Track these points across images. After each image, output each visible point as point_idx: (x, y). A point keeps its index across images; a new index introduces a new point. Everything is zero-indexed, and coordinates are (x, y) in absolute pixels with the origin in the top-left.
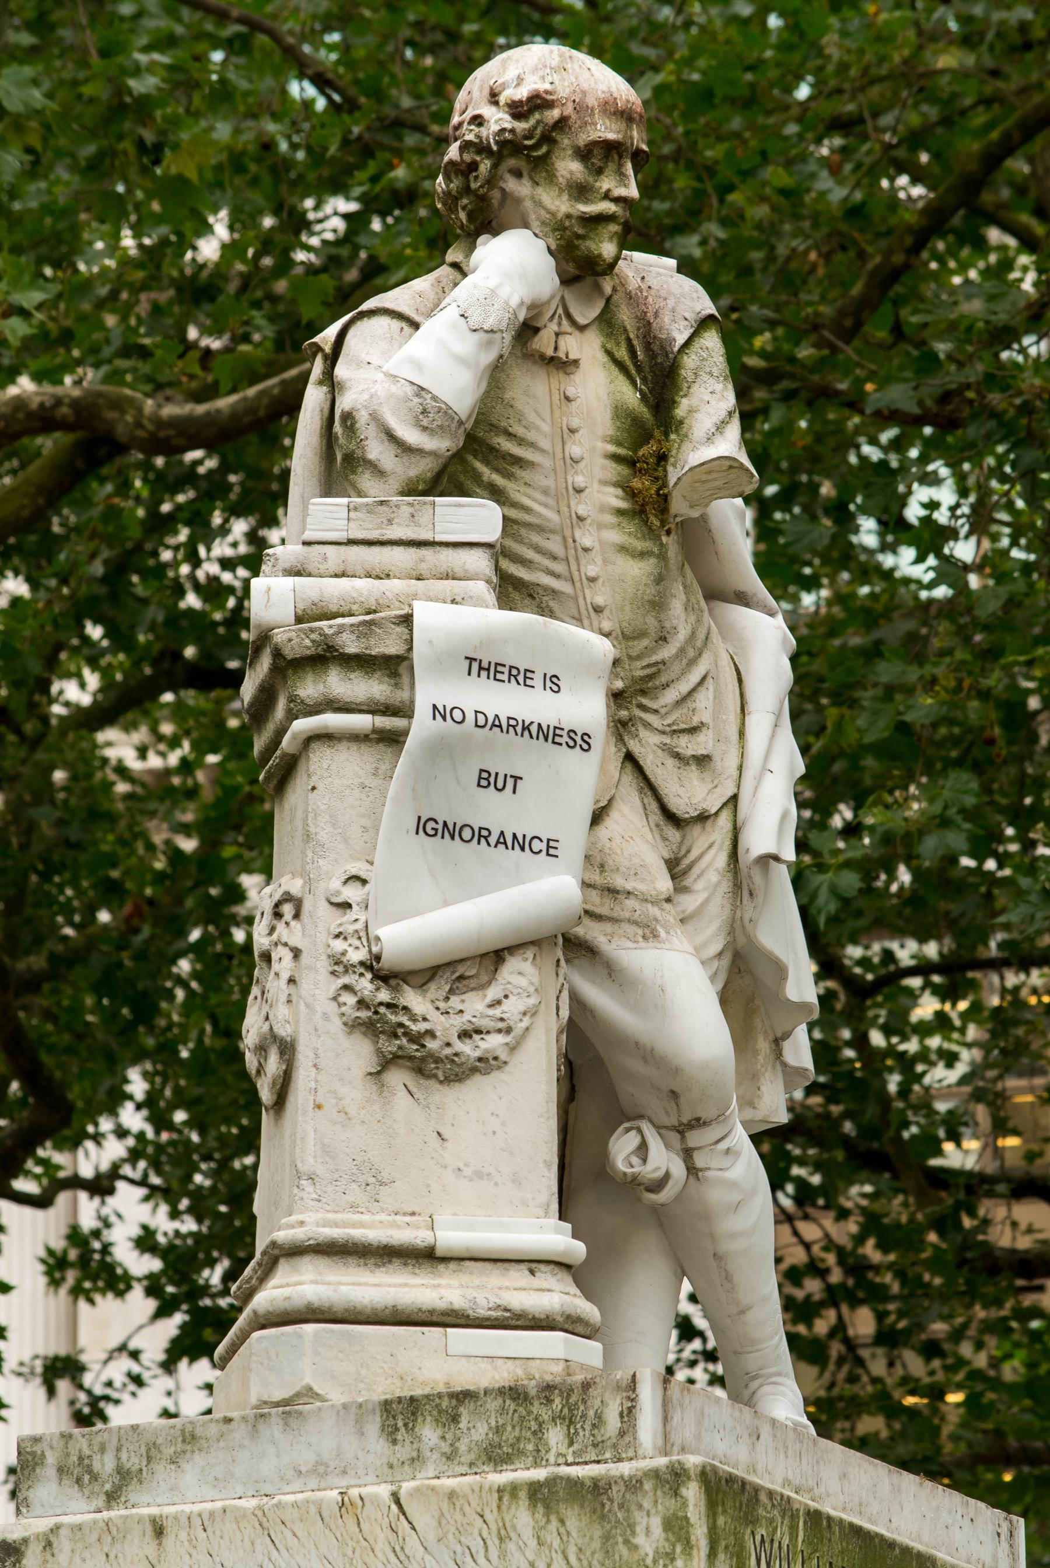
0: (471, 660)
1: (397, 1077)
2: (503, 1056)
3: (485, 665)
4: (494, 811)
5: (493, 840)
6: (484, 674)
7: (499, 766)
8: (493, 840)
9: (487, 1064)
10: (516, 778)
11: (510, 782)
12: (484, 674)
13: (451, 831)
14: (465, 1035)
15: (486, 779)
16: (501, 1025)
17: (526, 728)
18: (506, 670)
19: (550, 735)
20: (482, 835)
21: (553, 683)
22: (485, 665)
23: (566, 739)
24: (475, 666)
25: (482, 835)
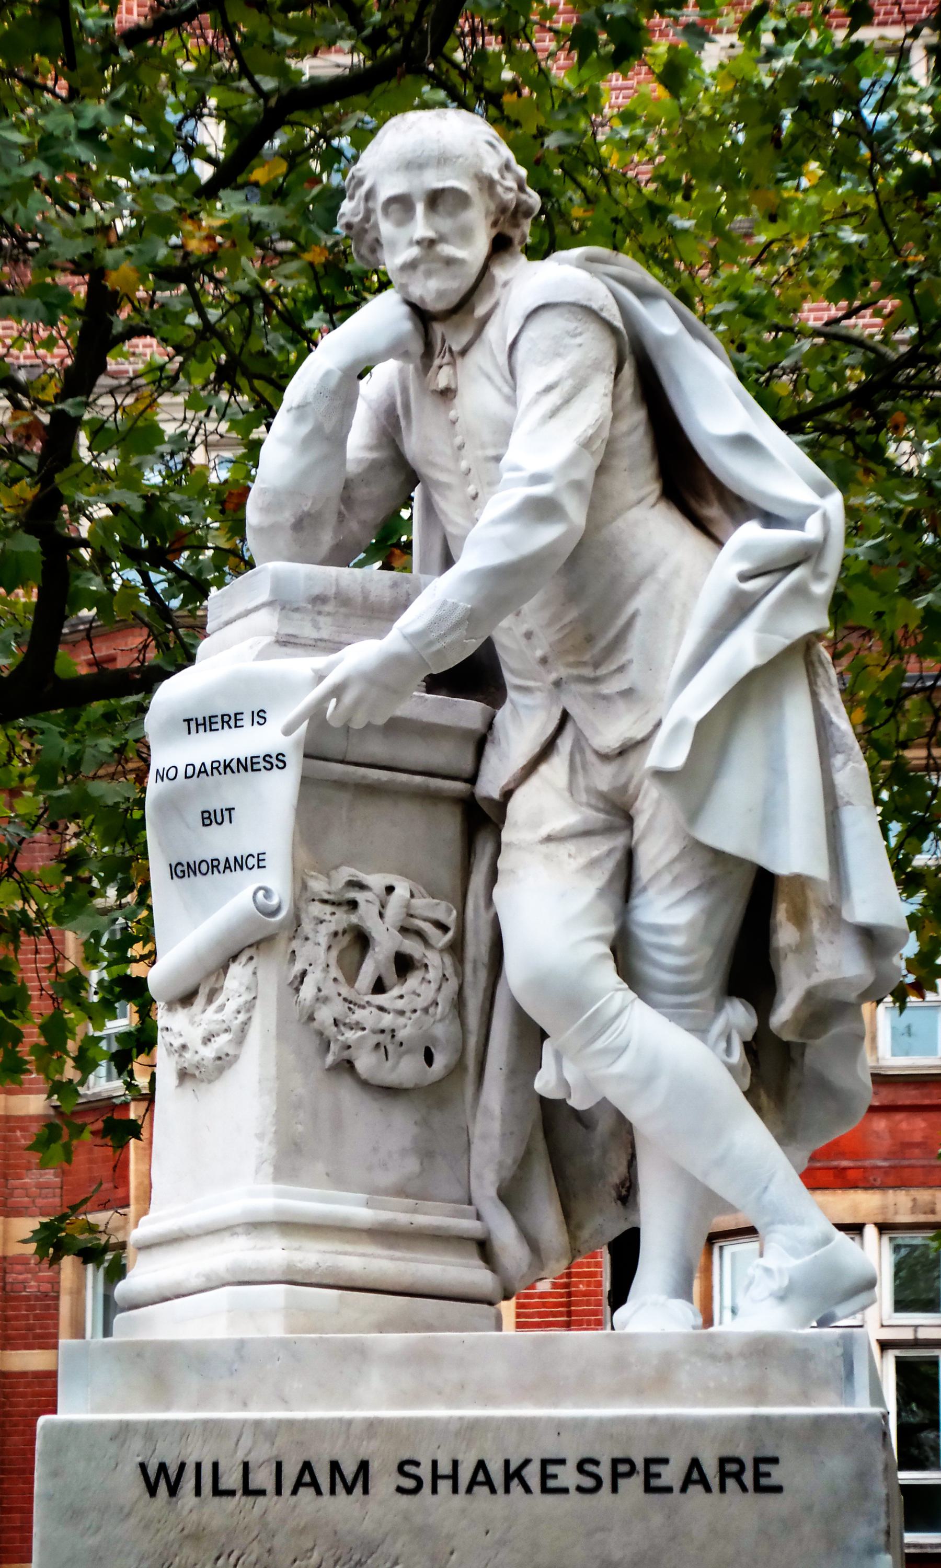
0: (188, 721)
1: (189, 1084)
2: (231, 1052)
3: (201, 721)
4: (219, 843)
5: (221, 867)
6: (201, 728)
7: (215, 804)
8: (221, 867)
9: (223, 1062)
10: (230, 810)
11: (226, 814)
12: (201, 728)
14: (207, 1040)
15: (208, 818)
16: (225, 1026)
17: (227, 766)
18: (219, 720)
19: (248, 765)
20: (214, 865)
21: (260, 716)
22: (201, 721)
23: (263, 764)
24: (193, 724)
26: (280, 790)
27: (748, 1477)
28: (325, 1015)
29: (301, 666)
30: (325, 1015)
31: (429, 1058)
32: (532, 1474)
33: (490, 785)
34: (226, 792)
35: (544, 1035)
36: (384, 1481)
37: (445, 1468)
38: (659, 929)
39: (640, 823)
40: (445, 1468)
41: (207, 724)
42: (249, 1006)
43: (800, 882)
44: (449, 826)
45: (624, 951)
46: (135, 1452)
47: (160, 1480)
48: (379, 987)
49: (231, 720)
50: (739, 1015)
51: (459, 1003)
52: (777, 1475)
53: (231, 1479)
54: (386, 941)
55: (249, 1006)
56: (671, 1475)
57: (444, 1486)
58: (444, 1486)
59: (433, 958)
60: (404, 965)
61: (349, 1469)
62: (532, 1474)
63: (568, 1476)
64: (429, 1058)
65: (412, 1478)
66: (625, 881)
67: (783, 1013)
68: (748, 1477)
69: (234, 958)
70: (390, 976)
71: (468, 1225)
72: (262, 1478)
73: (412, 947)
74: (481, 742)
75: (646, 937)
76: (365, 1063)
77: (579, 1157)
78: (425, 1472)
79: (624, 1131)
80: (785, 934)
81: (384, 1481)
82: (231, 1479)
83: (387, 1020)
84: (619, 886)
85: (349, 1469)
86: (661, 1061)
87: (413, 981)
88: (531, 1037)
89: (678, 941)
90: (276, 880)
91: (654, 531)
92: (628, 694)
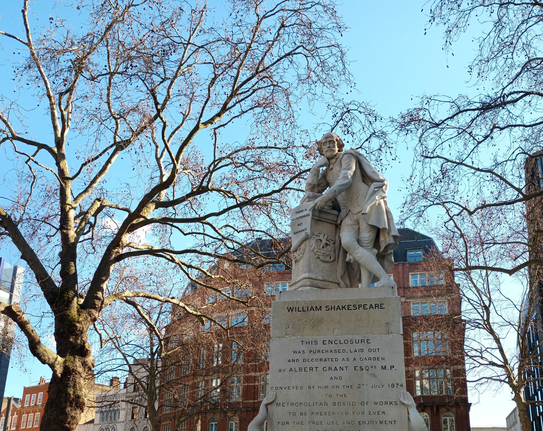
13: (297, 233)
15: (299, 225)
20: (300, 231)
25: (300, 231)
26: (309, 219)
27: (379, 307)
28: (315, 250)
29: (312, 202)
30: (315, 250)
31: (331, 258)
32: (346, 307)
33: (339, 222)
34: (301, 221)
35: (347, 253)
36: (324, 309)
37: (333, 307)
38: (364, 238)
39: (360, 224)
40: (333, 307)
41: (299, 212)
42: (304, 249)
43: (385, 229)
44: (334, 227)
45: (359, 241)
46: (287, 305)
47: (290, 309)
48: (323, 247)
49: (302, 211)
50: (375, 251)
51: (335, 251)
52: (383, 306)
53: (301, 309)
54: (324, 241)
55: (304, 249)
56: (368, 307)
57: (333, 309)
58: (333, 309)
59: (331, 244)
60: (327, 244)
61: (318, 307)
62: (346, 307)
63: (351, 307)
64: (331, 258)
65: (328, 308)
66: (358, 231)
67: (382, 250)
68: (379, 307)
69: (303, 243)
70: (325, 245)
71: (337, 282)
72: (305, 309)
73: (327, 242)
74: (338, 216)
75: (362, 239)
76: (321, 257)
77: (352, 272)
78: (330, 308)
79: (359, 265)
80: (382, 238)
81: (324, 309)
82: (301, 309)
83: (324, 252)
84: (357, 232)
85: (318, 307)
86: (365, 256)
87: (328, 247)
88: (345, 252)
89: (367, 239)
90: (308, 231)
91: (362, 186)
92: (358, 205)
